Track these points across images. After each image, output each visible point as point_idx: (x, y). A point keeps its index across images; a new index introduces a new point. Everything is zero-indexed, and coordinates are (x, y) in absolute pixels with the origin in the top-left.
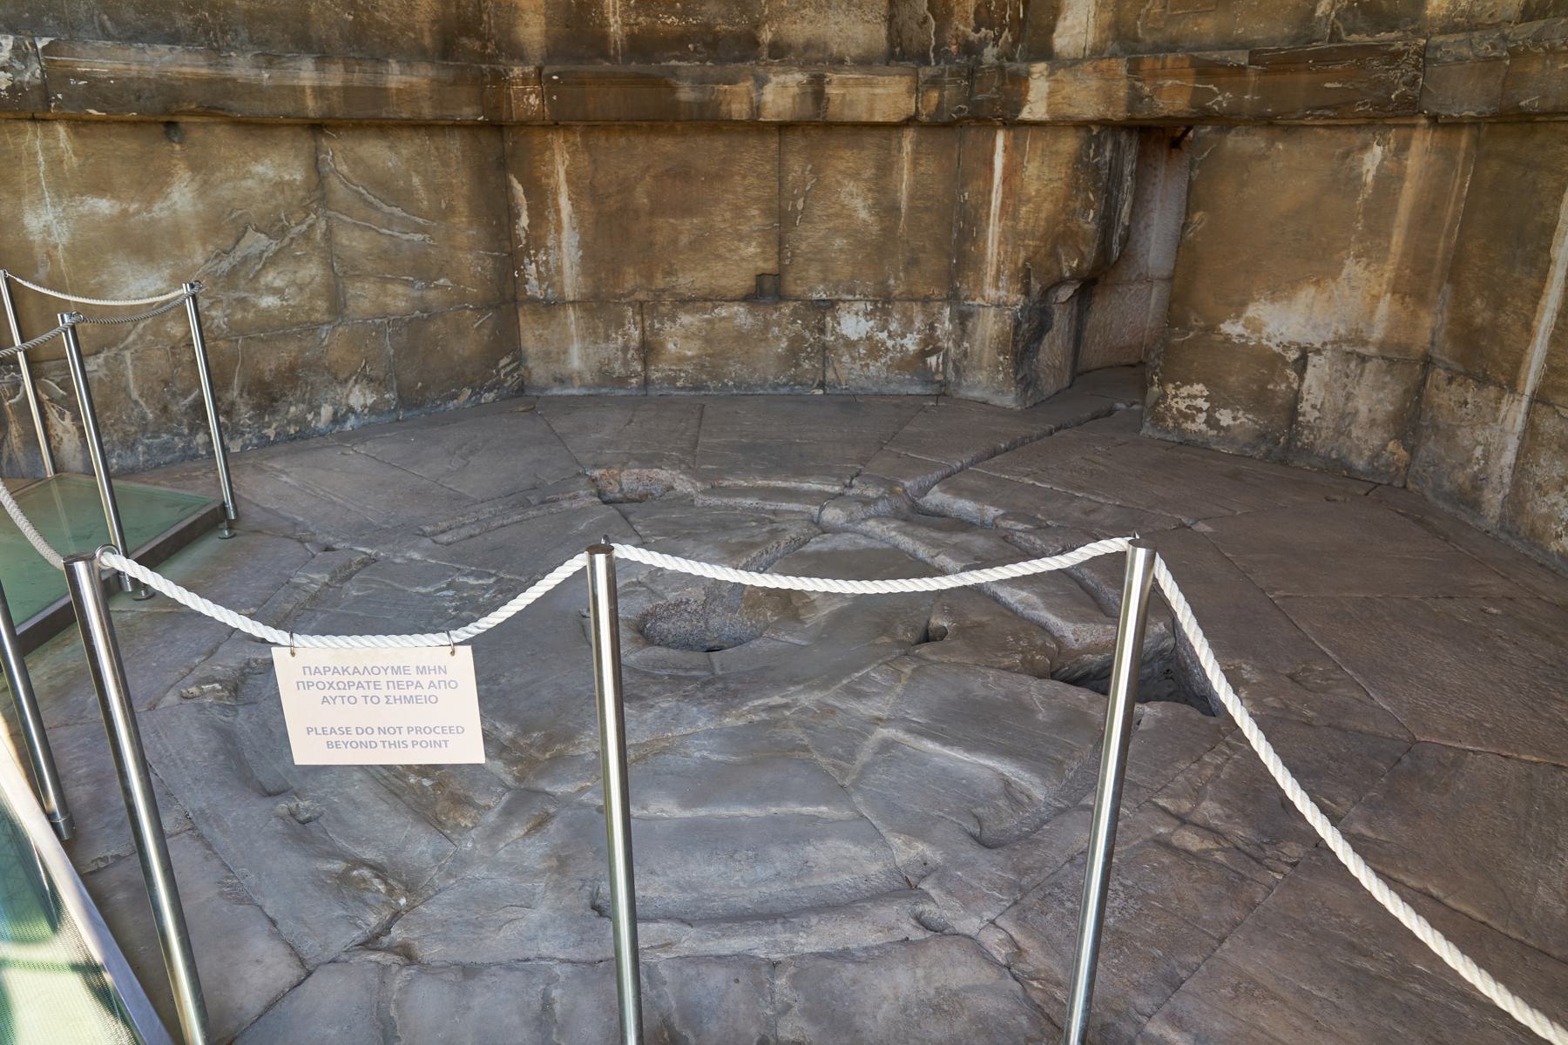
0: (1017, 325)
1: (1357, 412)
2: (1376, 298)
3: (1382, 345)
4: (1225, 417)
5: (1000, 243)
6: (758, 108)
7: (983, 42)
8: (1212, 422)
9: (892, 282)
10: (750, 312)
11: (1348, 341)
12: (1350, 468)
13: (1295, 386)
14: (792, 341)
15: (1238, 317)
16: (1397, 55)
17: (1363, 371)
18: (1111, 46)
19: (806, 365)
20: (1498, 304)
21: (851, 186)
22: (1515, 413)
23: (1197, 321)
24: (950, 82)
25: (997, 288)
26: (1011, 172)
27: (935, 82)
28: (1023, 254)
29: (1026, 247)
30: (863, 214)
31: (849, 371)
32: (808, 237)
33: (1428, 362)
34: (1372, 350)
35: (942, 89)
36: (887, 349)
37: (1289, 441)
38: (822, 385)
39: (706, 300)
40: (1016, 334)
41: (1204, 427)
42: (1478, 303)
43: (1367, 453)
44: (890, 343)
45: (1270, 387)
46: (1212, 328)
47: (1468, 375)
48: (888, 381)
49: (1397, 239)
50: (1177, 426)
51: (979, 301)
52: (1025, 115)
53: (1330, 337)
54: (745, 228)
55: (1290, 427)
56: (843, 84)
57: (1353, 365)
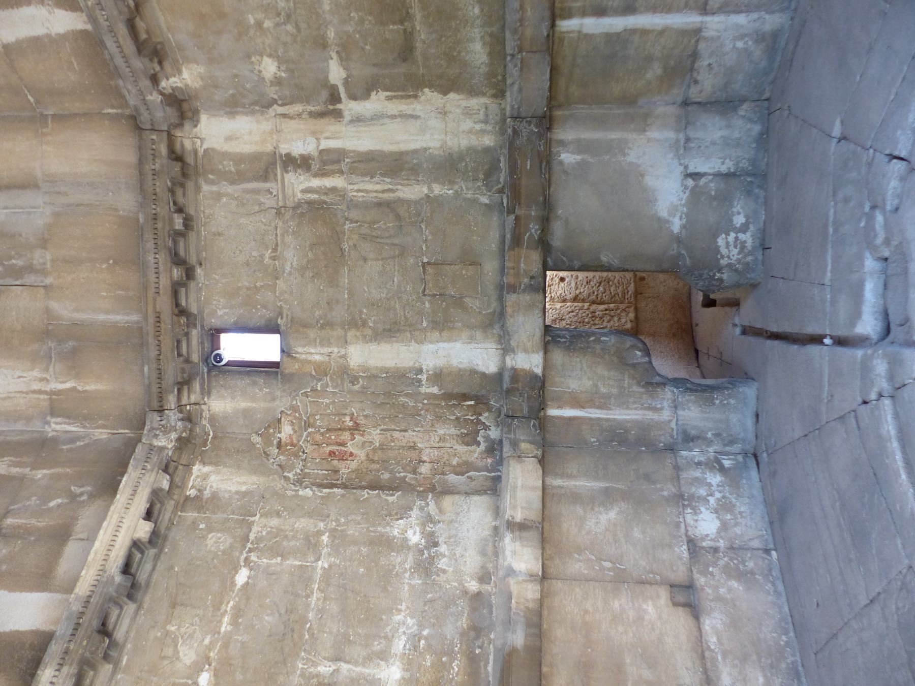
0: (691, 390)
1: (722, 137)
2: (649, 140)
3: (678, 131)
4: (739, 220)
5: (628, 408)
6: (531, 576)
7: (487, 438)
8: (744, 229)
9: (665, 493)
10: (709, 614)
11: (677, 150)
12: (761, 134)
13: (710, 177)
14: (730, 576)
15: (668, 222)
16: (515, 132)
17: (695, 139)
18: (496, 330)
19: (751, 564)
20: (649, 59)
21: (590, 524)
22: (714, 23)
23: (674, 250)
24: (515, 435)
25: (662, 409)
26: (577, 403)
27: (515, 444)
28: (635, 388)
29: (630, 386)
30: (612, 514)
31: (750, 526)
32: (635, 560)
33: (686, 103)
34: (682, 136)
35: (520, 440)
36: (724, 497)
37: (748, 174)
38: (767, 551)
39: (703, 657)
40: (696, 391)
41: (749, 234)
42: (649, 76)
43: (749, 126)
44: (718, 495)
45: (713, 193)
46: (678, 239)
47: (692, 69)
48: (751, 497)
49: (614, 135)
50: (751, 253)
51: (673, 425)
52: (539, 371)
53: (676, 162)
54: (632, 614)
55: (740, 176)
56: (514, 507)
57: (693, 145)
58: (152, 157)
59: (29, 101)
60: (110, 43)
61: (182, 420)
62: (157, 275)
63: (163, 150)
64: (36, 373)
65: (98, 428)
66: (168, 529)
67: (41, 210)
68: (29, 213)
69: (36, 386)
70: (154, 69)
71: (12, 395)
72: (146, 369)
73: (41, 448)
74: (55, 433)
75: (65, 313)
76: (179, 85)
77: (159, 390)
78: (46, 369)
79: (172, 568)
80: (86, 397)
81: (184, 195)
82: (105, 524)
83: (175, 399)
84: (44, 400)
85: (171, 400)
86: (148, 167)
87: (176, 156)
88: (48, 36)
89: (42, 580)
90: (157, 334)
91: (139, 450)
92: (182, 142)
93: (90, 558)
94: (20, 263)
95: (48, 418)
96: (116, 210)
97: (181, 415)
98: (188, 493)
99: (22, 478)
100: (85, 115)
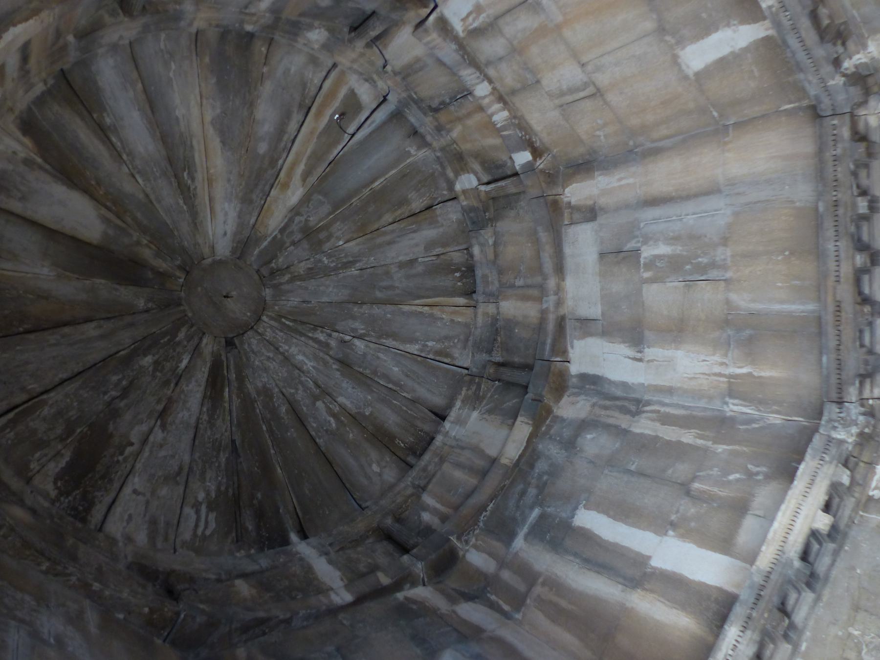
58: (832, 143)
59: (713, 117)
60: (793, 42)
61: (864, 414)
62: (837, 263)
63: (846, 133)
64: (717, 358)
65: (772, 412)
66: (848, 526)
67: (722, 212)
68: (713, 215)
69: (717, 369)
70: (837, 53)
71: (697, 376)
72: (824, 359)
73: (721, 425)
74: (732, 414)
75: (743, 304)
76: (863, 61)
77: (838, 381)
78: (726, 355)
79: (853, 568)
80: (761, 382)
81: (868, 176)
82: (783, 507)
83: (857, 392)
84: (723, 382)
85: (852, 393)
86: (828, 155)
87: (860, 137)
88: (732, 53)
89: (724, 543)
90: (838, 323)
91: (817, 440)
92: (866, 120)
93: (770, 535)
94: (704, 260)
95: (727, 399)
96: (792, 202)
97: (863, 409)
98: (871, 493)
99: (706, 450)
100: (763, 116)
